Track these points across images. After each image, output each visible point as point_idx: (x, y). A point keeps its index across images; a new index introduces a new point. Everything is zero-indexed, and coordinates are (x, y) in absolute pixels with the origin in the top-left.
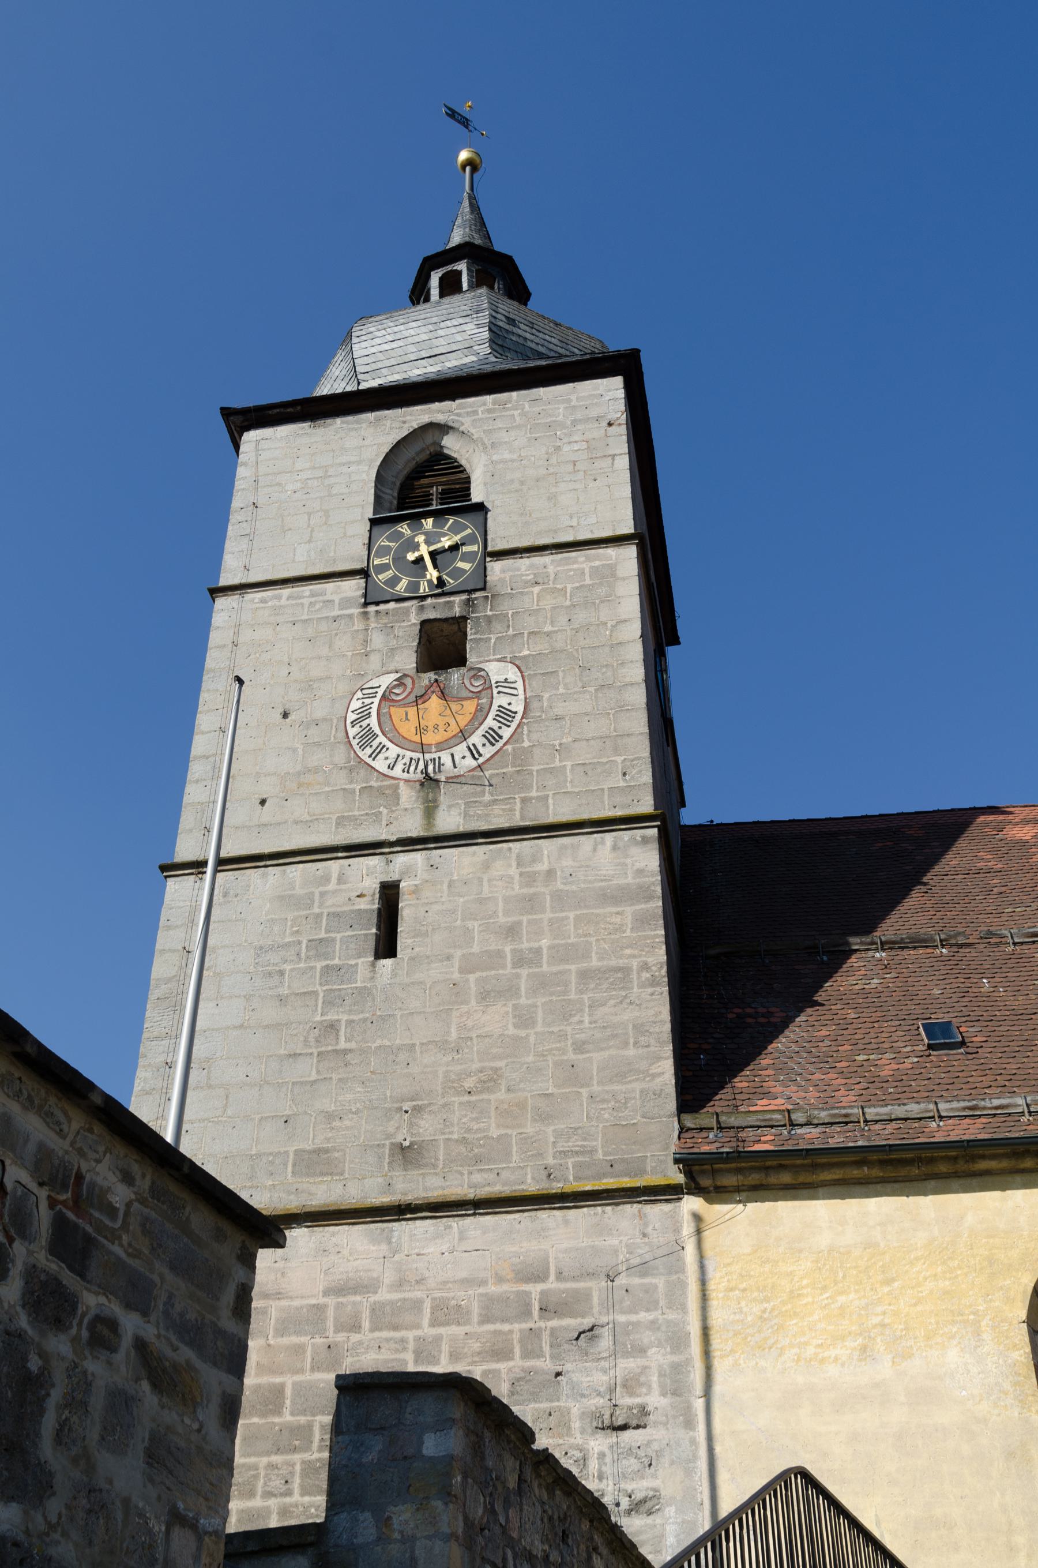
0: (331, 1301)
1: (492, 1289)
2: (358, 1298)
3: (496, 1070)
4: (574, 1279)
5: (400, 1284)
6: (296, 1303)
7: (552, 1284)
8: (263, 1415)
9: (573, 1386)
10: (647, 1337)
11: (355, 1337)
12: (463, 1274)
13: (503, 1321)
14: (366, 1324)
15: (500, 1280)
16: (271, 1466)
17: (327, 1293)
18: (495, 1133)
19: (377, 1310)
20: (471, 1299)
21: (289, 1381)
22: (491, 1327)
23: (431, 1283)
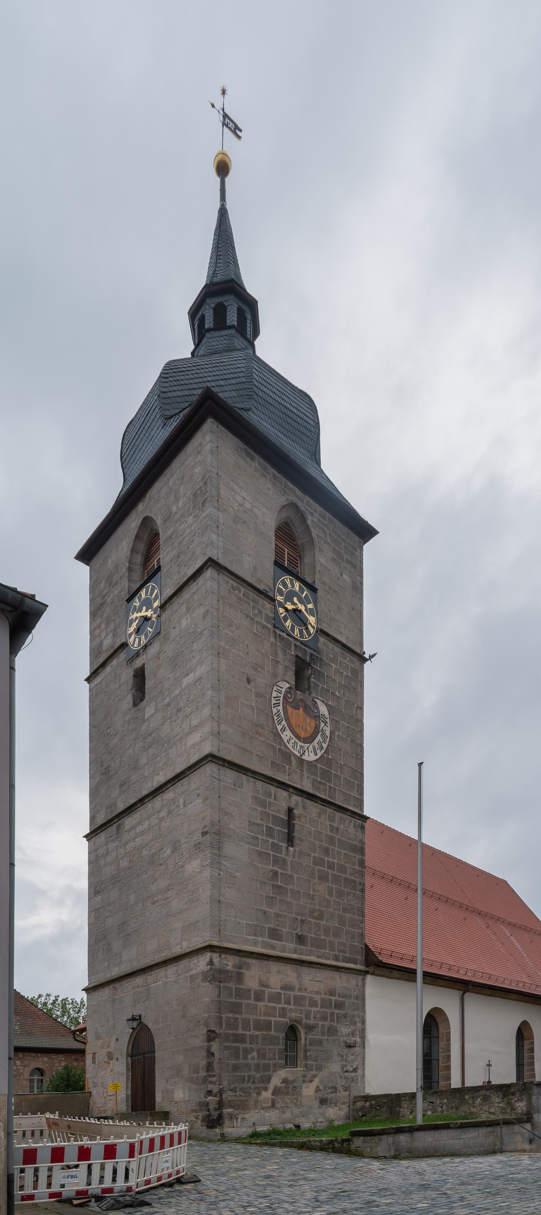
0: (283, 992)
1: (323, 996)
2: (289, 992)
3: (323, 911)
4: (342, 997)
5: (300, 990)
6: (273, 991)
7: (337, 998)
8: (266, 1031)
9: (341, 1032)
10: (357, 1019)
11: (290, 1007)
12: (316, 990)
13: (326, 1008)
14: (292, 1002)
15: (325, 994)
16: (270, 1049)
17: (282, 988)
18: (323, 937)
19: (295, 997)
20: (317, 998)
21: (273, 1019)
22: (323, 1010)
23: (308, 991)
